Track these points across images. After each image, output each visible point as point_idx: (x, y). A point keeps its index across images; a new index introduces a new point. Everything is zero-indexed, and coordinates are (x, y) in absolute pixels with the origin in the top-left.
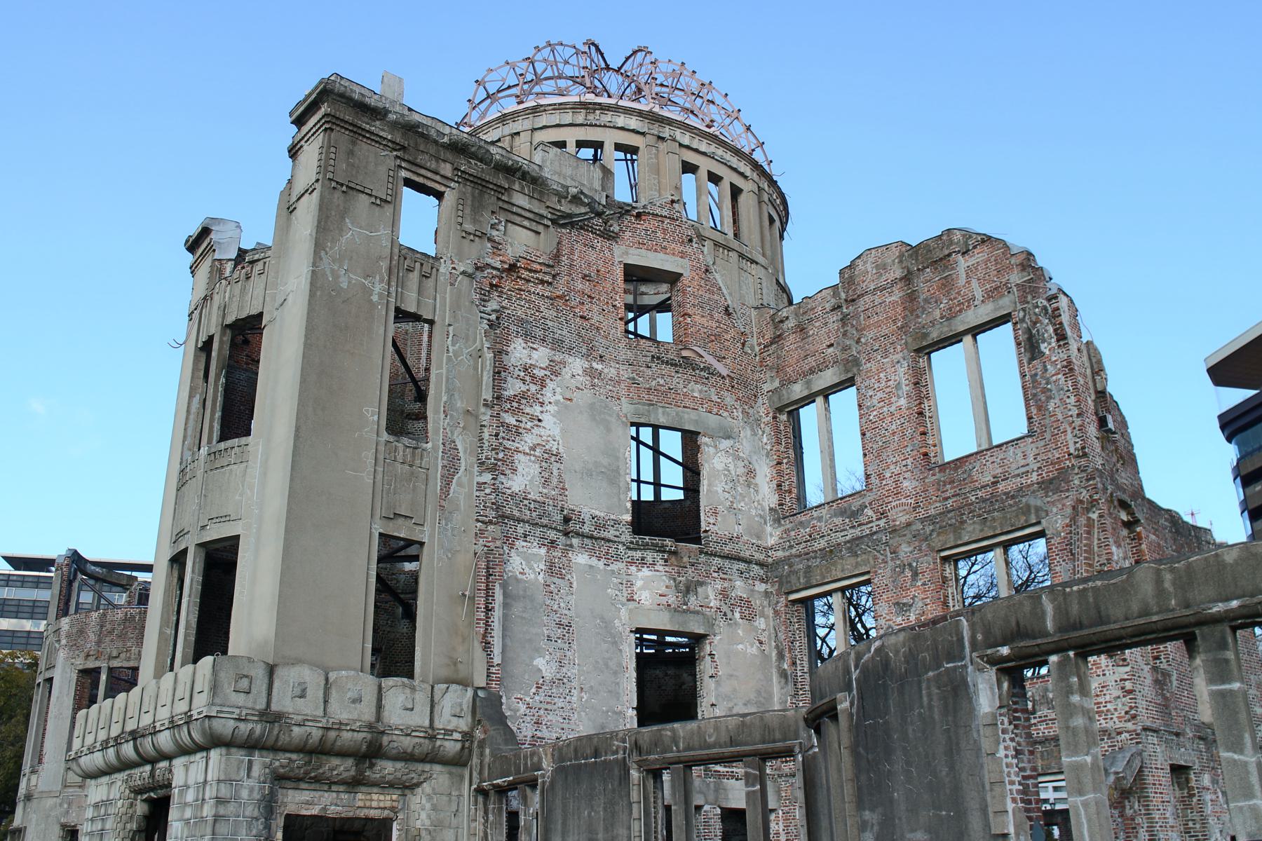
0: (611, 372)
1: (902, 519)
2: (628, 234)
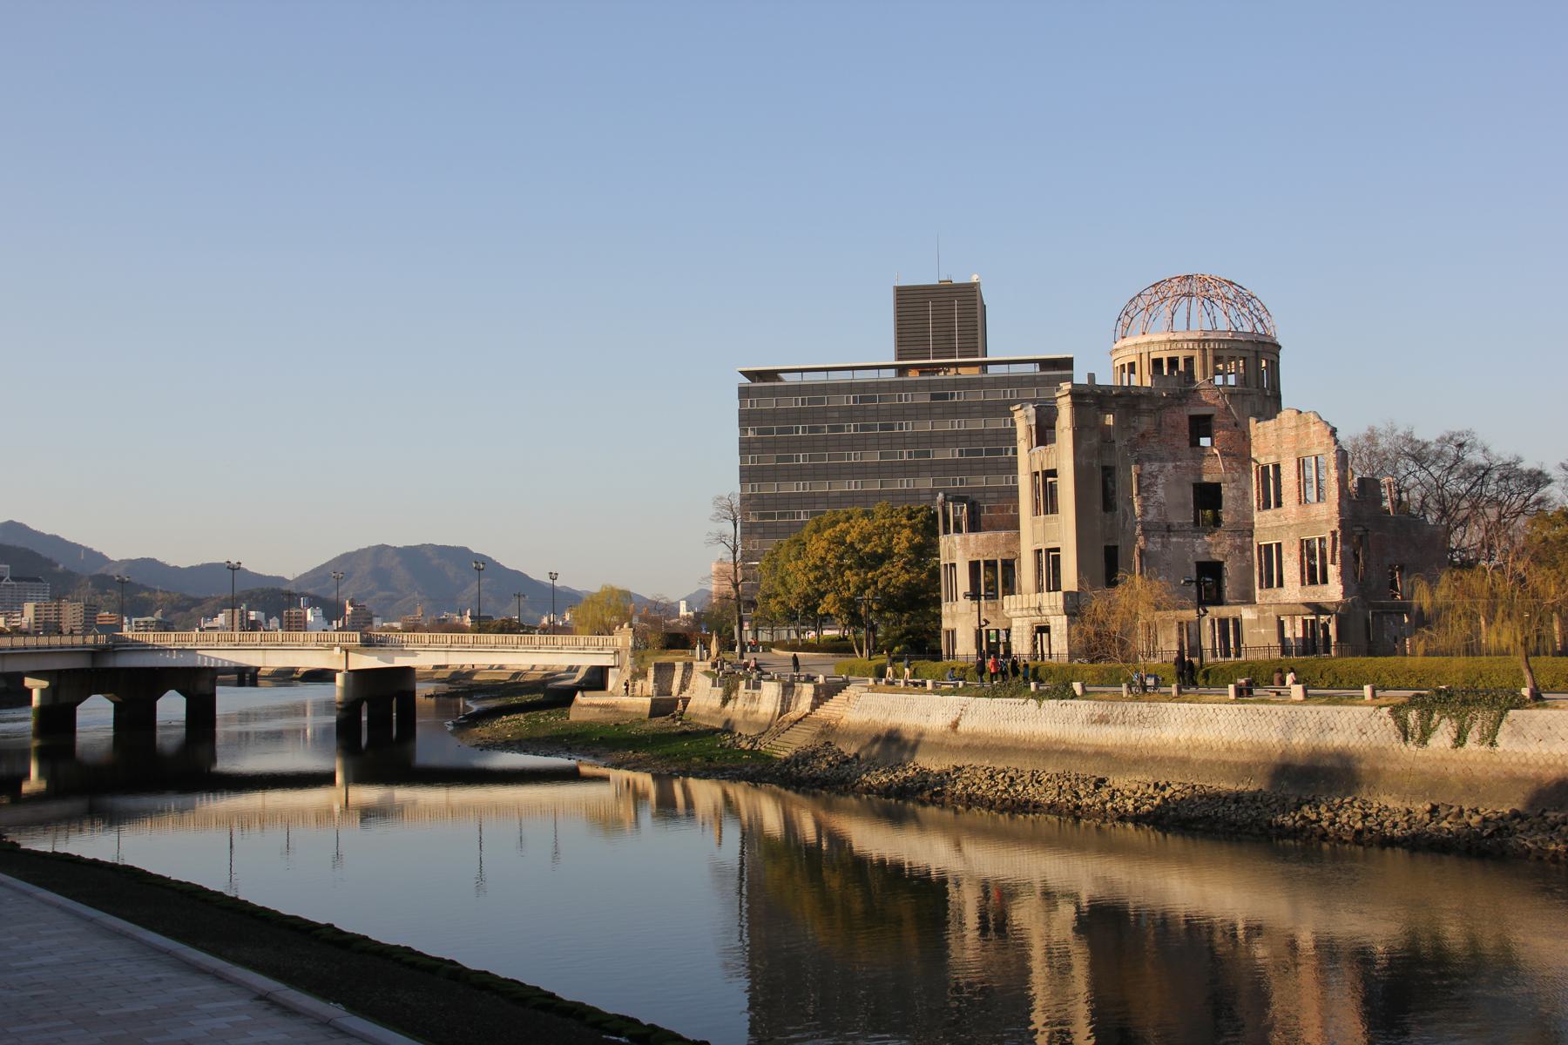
0: (1184, 464)
1: (1292, 522)
2: (1190, 401)
